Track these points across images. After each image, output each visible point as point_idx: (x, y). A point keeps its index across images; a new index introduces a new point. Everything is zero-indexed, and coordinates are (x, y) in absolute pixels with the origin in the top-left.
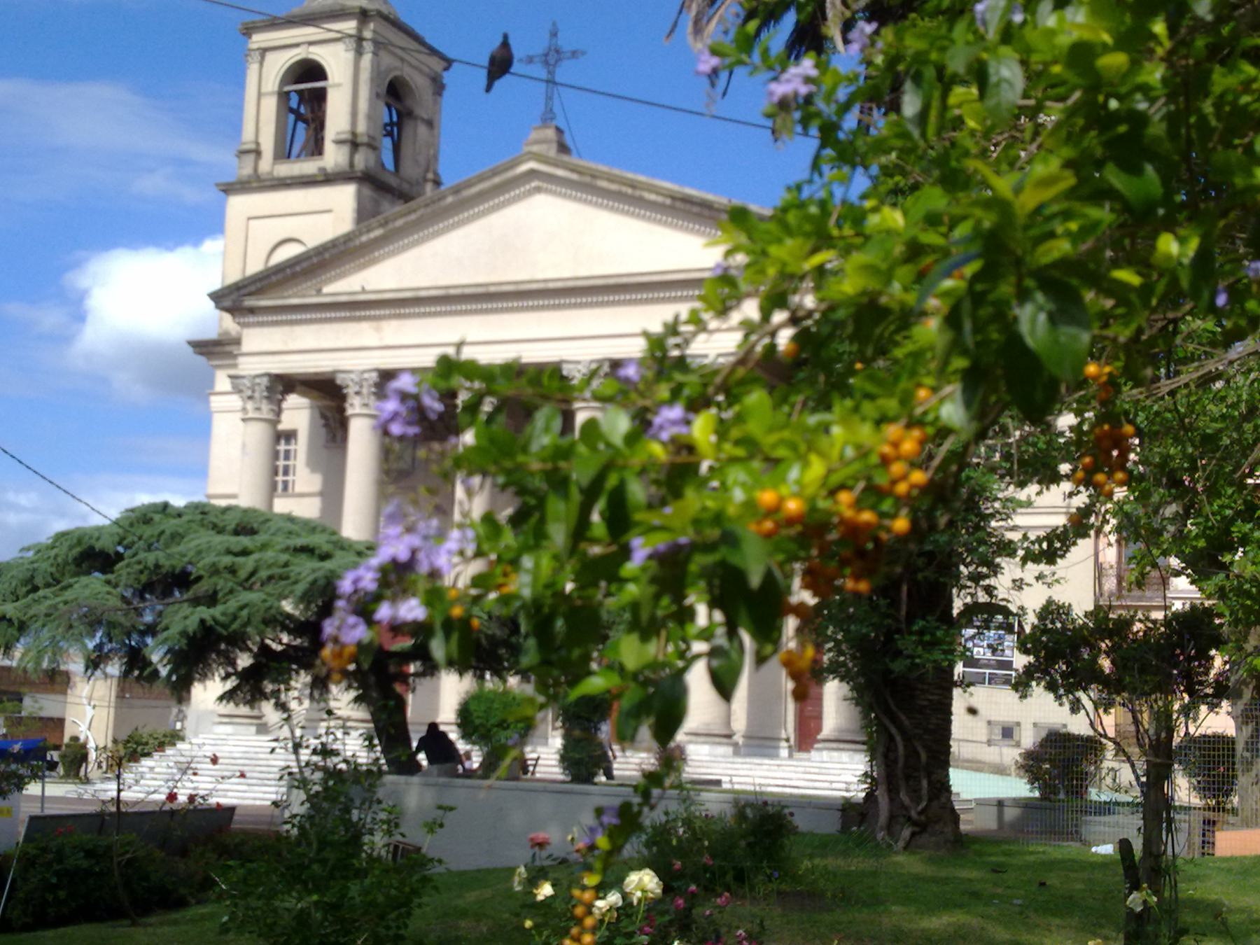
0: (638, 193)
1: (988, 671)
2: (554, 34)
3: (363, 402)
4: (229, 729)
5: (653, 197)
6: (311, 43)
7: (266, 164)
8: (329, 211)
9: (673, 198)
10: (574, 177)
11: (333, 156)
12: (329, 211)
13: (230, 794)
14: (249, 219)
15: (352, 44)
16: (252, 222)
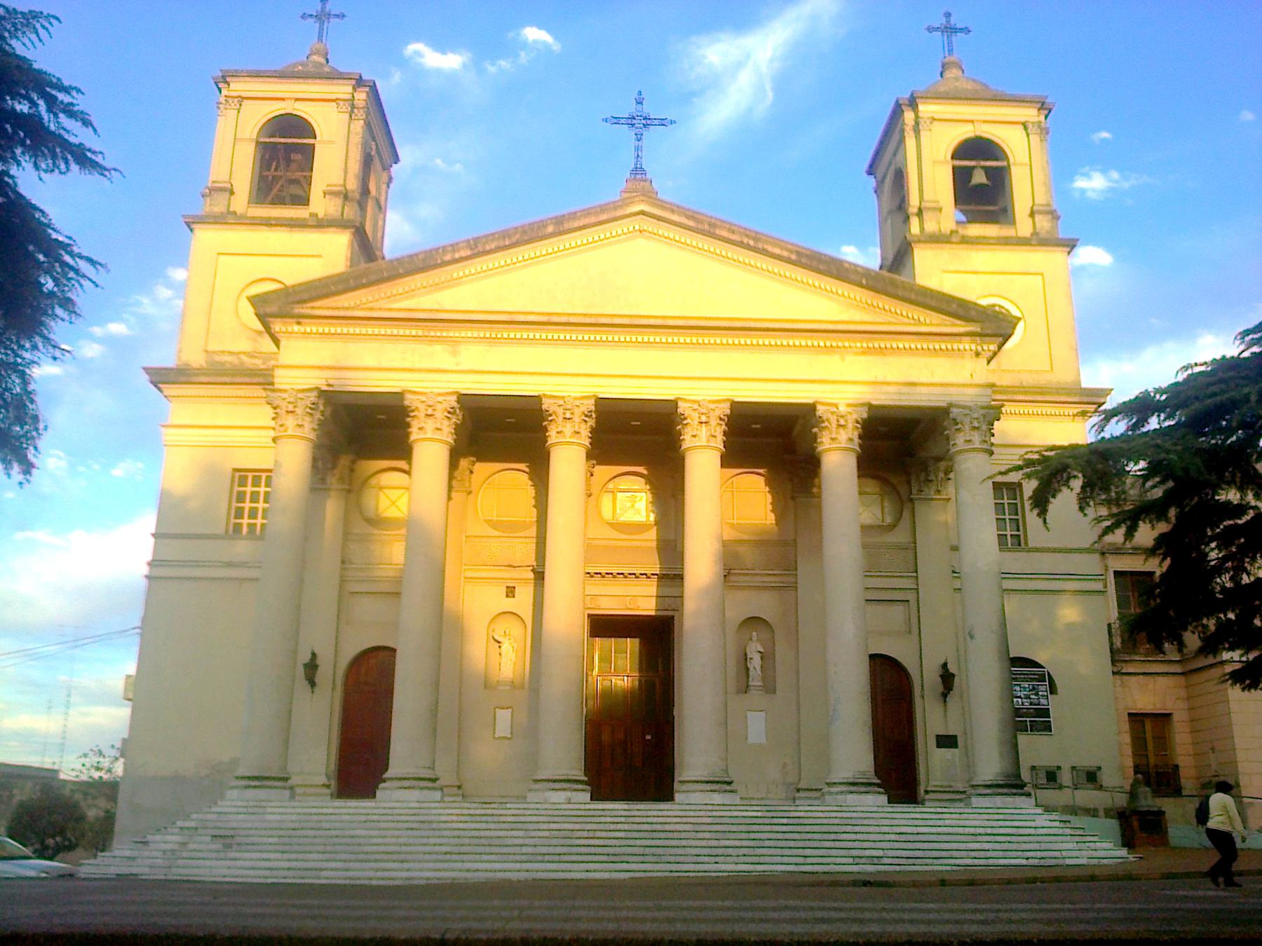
0: (760, 246)
1: (1028, 719)
2: (639, 102)
3: (435, 426)
4: (261, 794)
5: (777, 251)
6: (297, 99)
7: (240, 201)
8: (319, 256)
9: (798, 253)
10: (691, 223)
11: (320, 204)
12: (319, 256)
13: (324, 873)
14: (219, 254)
15: (346, 107)
16: (222, 258)
